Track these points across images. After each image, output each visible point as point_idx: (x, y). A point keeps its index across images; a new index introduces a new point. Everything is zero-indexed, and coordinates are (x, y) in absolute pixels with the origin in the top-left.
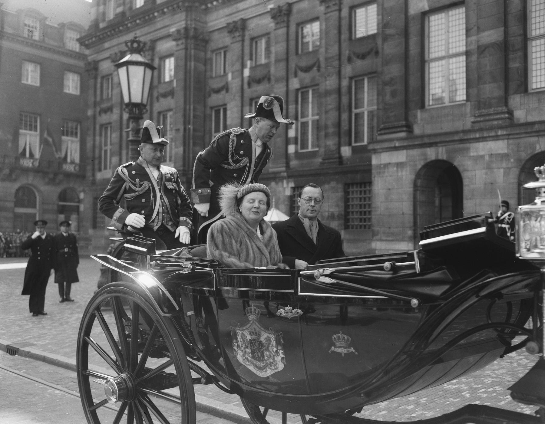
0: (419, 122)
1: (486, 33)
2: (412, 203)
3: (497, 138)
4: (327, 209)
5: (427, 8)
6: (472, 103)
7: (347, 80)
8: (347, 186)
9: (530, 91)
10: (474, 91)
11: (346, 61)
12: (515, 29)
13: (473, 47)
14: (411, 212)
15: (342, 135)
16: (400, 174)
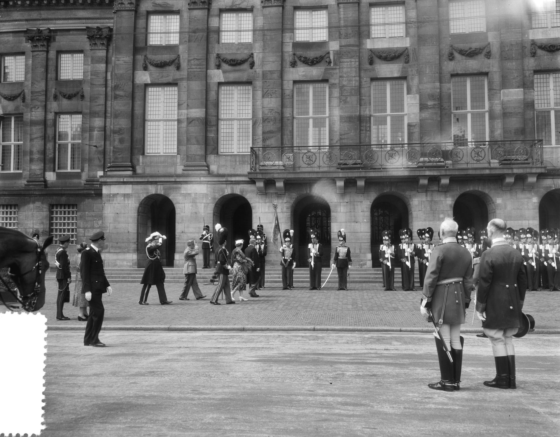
0: (141, 164)
1: (193, 110)
2: (136, 224)
3: (200, 183)
4: (31, 226)
5: (149, 82)
6: (182, 156)
7: (53, 114)
8: (52, 206)
9: (220, 153)
10: (184, 148)
11: (52, 98)
12: (212, 111)
13: (184, 117)
14: (136, 231)
15: (47, 162)
16: (126, 202)
